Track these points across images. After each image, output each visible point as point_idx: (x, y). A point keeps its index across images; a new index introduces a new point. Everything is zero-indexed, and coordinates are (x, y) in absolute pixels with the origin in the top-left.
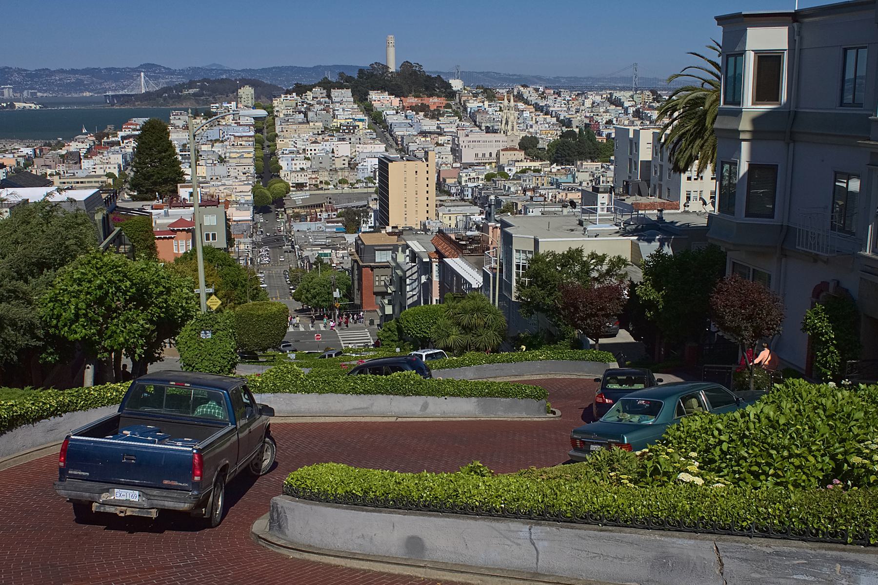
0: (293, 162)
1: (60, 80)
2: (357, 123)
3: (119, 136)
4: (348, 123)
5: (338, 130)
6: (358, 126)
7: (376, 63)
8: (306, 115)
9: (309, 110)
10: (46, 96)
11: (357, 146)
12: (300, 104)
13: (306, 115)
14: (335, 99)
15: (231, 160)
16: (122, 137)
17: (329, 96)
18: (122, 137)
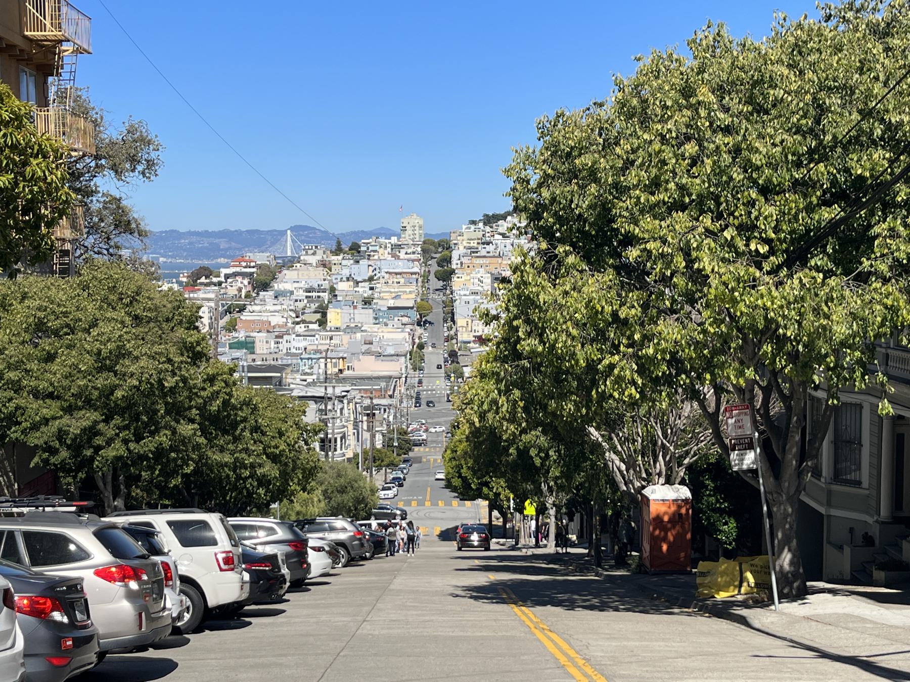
1: (190, 243)
3: (222, 275)
10: (171, 262)
12: (489, 235)
15: (380, 302)
16: (225, 275)
18: (225, 275)
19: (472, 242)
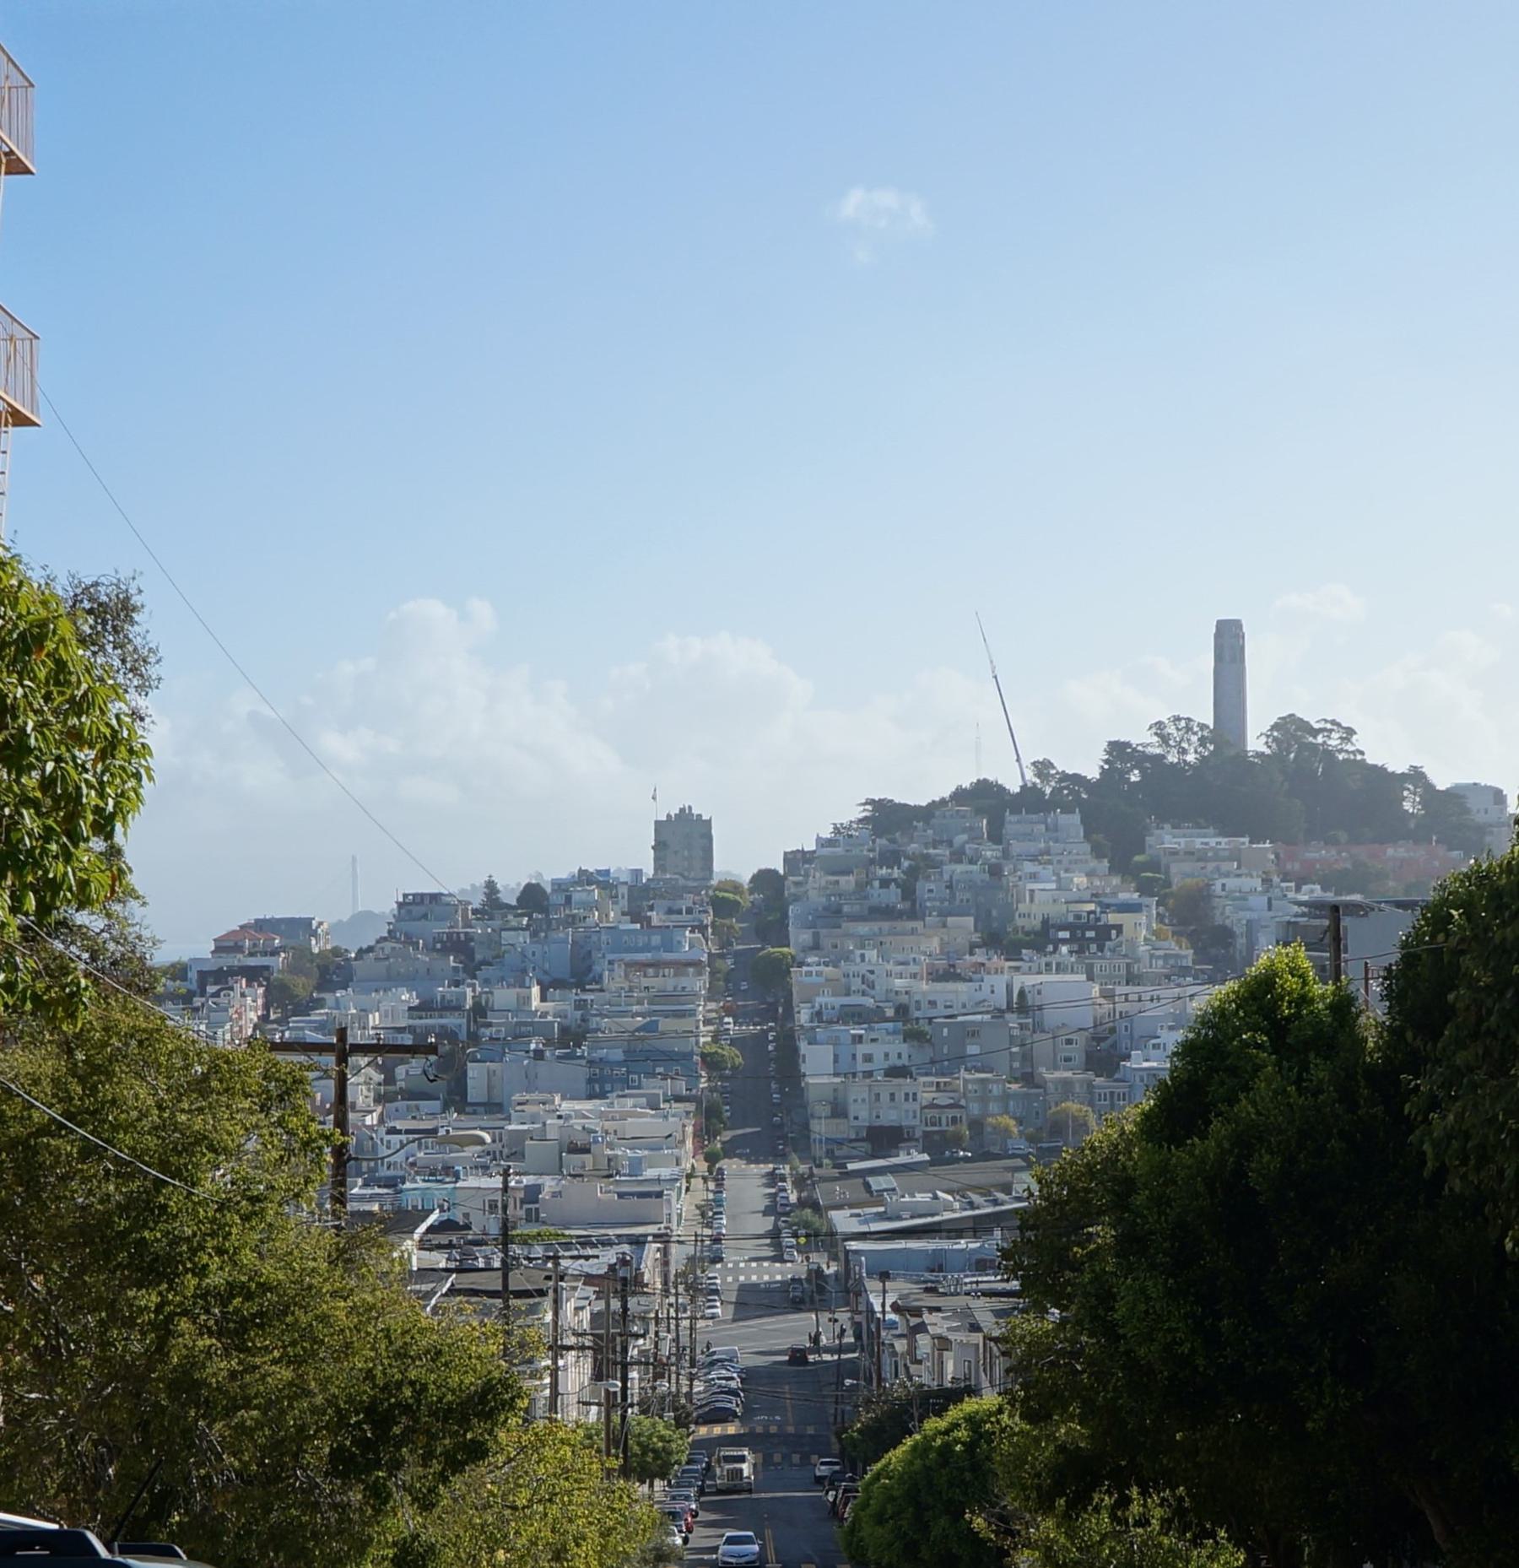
0: (862, 1049)
2: (1112, 918)
4: (1078, 917)
5: (1042, 938)
6: (1119, 928)
7: (1177, 719)
8: (908, 892)
9: (927, 878)
11: (1121, 990)
13: (908, 892)
14: (1017, 847)
17: (996, 837)
19: (843, 879)
